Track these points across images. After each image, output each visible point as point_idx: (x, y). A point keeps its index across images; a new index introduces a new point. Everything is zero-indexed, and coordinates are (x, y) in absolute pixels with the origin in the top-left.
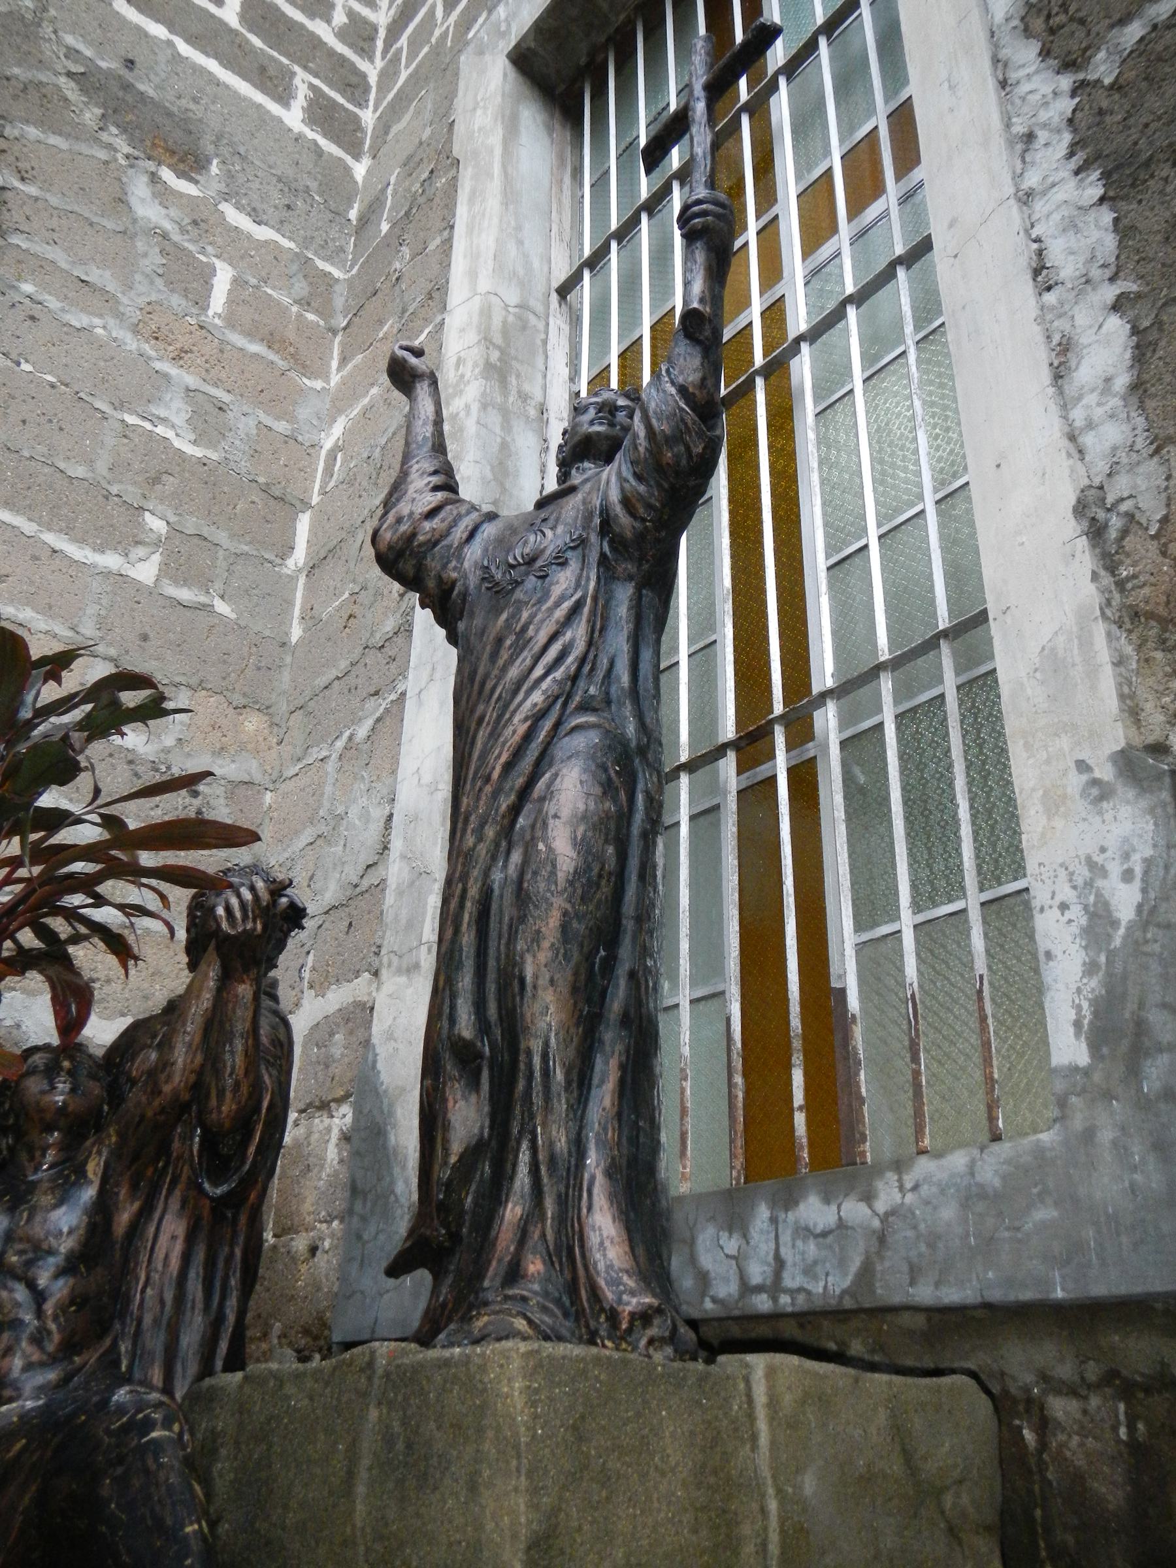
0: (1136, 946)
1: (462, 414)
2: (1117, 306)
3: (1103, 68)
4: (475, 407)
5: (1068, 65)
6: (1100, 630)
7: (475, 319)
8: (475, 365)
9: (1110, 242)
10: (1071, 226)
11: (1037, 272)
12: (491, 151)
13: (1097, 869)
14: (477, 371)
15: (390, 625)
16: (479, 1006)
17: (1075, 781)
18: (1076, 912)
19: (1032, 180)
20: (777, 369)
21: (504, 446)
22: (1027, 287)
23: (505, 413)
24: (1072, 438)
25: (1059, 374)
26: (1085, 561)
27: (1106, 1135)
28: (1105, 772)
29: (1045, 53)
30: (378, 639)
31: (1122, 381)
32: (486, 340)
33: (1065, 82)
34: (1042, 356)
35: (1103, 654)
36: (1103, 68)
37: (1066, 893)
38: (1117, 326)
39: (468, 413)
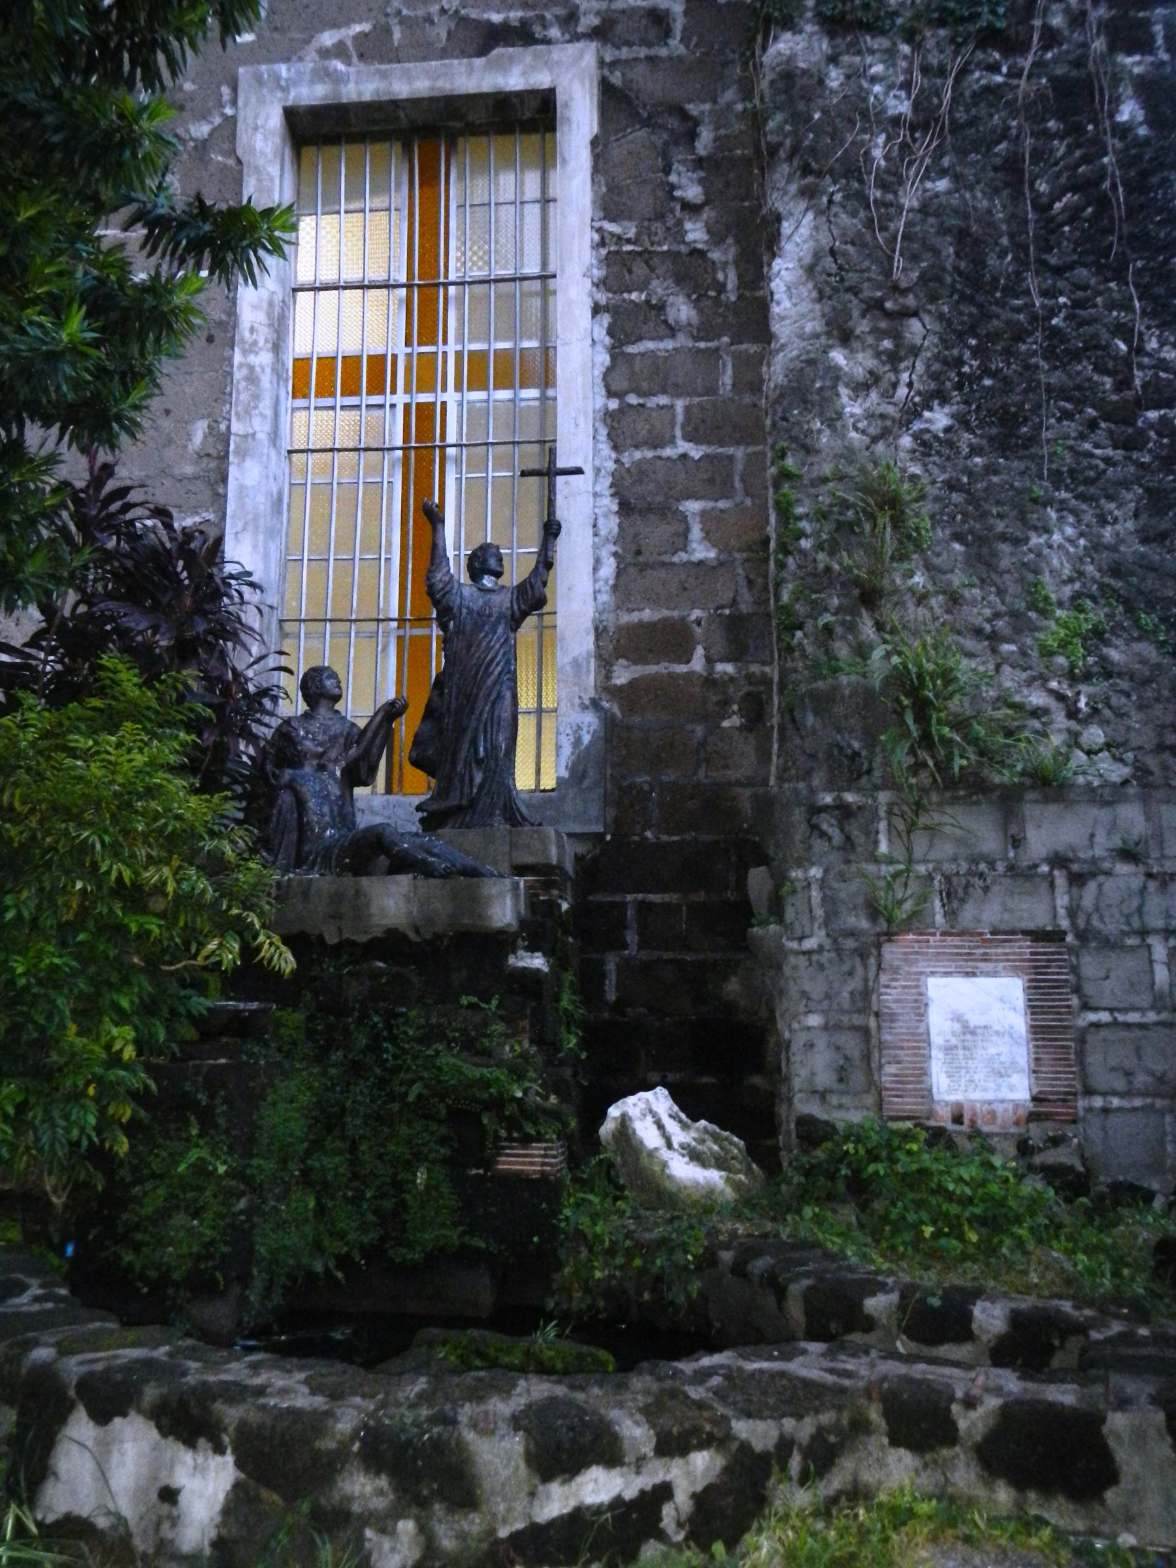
0: (587, 748)
1: (258, 369)
2: (615, 554)
3: (626, 459)
4: (268, 370)
5: (615, 448)
6: (593, 661)
7: (265, 305)
8: (266, 341)
9: (616, 530)
10: (605, 516)
11: (595, 526)
12: (272, 179)
13: (579, 728)
14: (269, 346)
15: (189, 470)
16: (486, 749)
17: (577, 701)
18: (572, 738)
19: (598, 489)
20: (443, 448)
21: (277, 397)
22: (590, 532)
23: (279, 377)
24: (595, 592)
25: (595, 569)
26: (592, 638)
27: (571, 796)
28: (587, 702)
29: (609, 435)
30: (176, 472)
31: (611, 582)
32: (271, 325)
33: (614, 455)
34: (592, 561)
35: (592, 667)
36: (626, 459)
37: (569, 731)
38: (612, 560)
39: (263, 371)
